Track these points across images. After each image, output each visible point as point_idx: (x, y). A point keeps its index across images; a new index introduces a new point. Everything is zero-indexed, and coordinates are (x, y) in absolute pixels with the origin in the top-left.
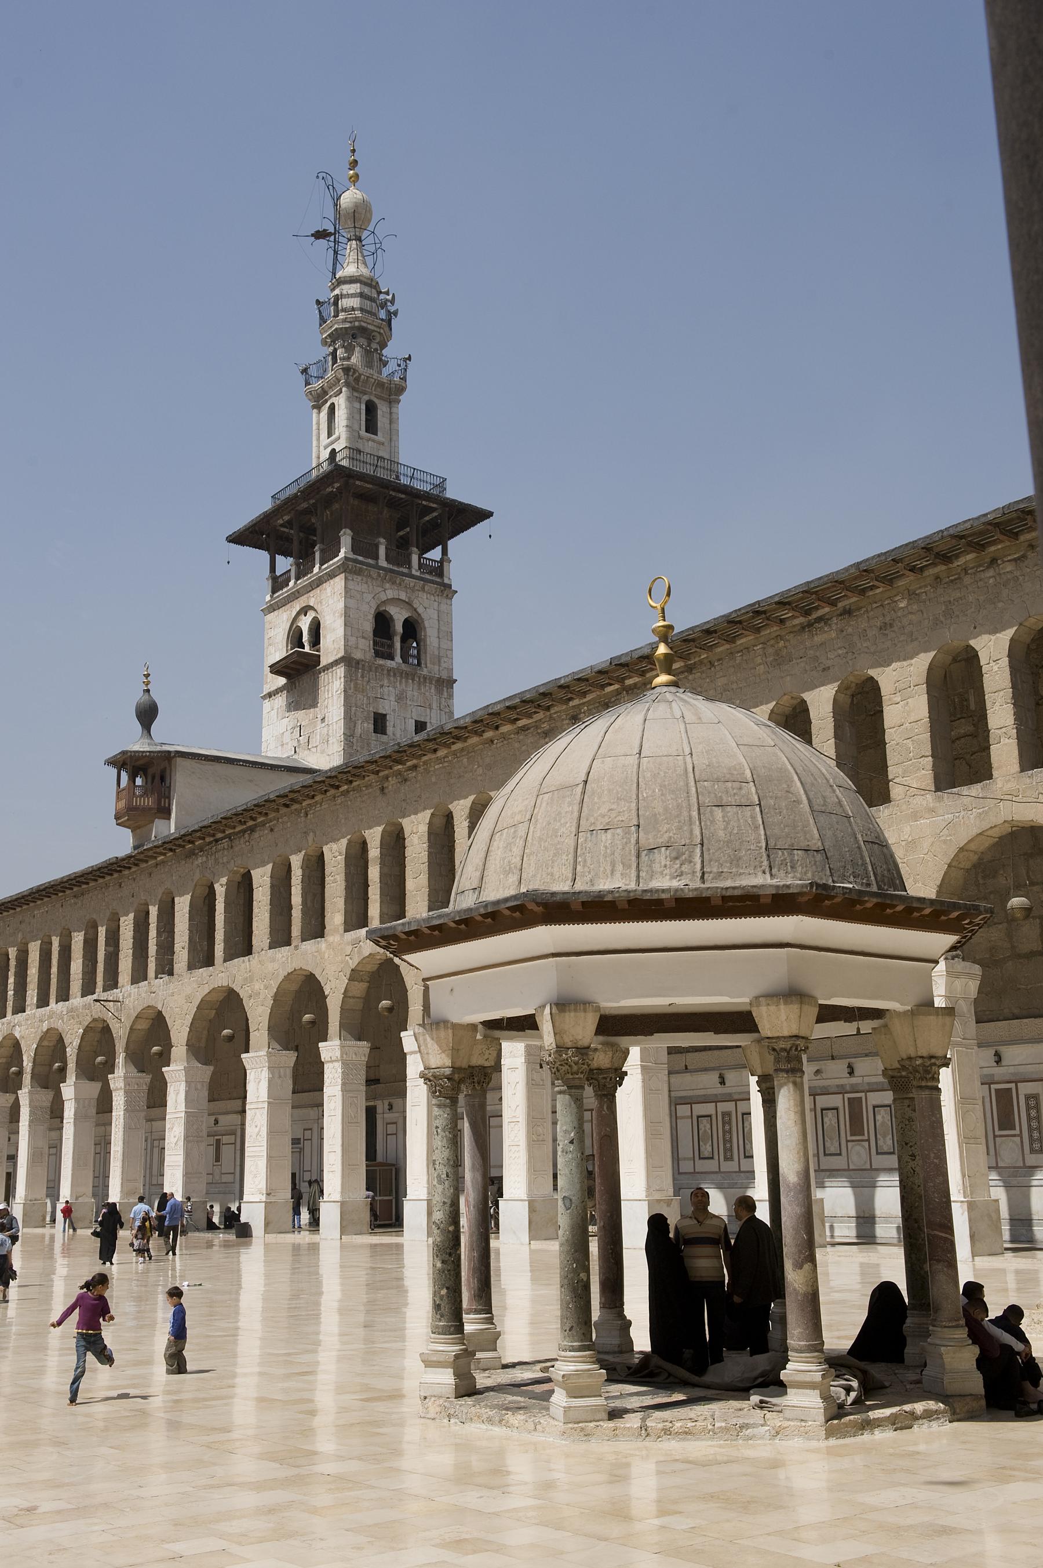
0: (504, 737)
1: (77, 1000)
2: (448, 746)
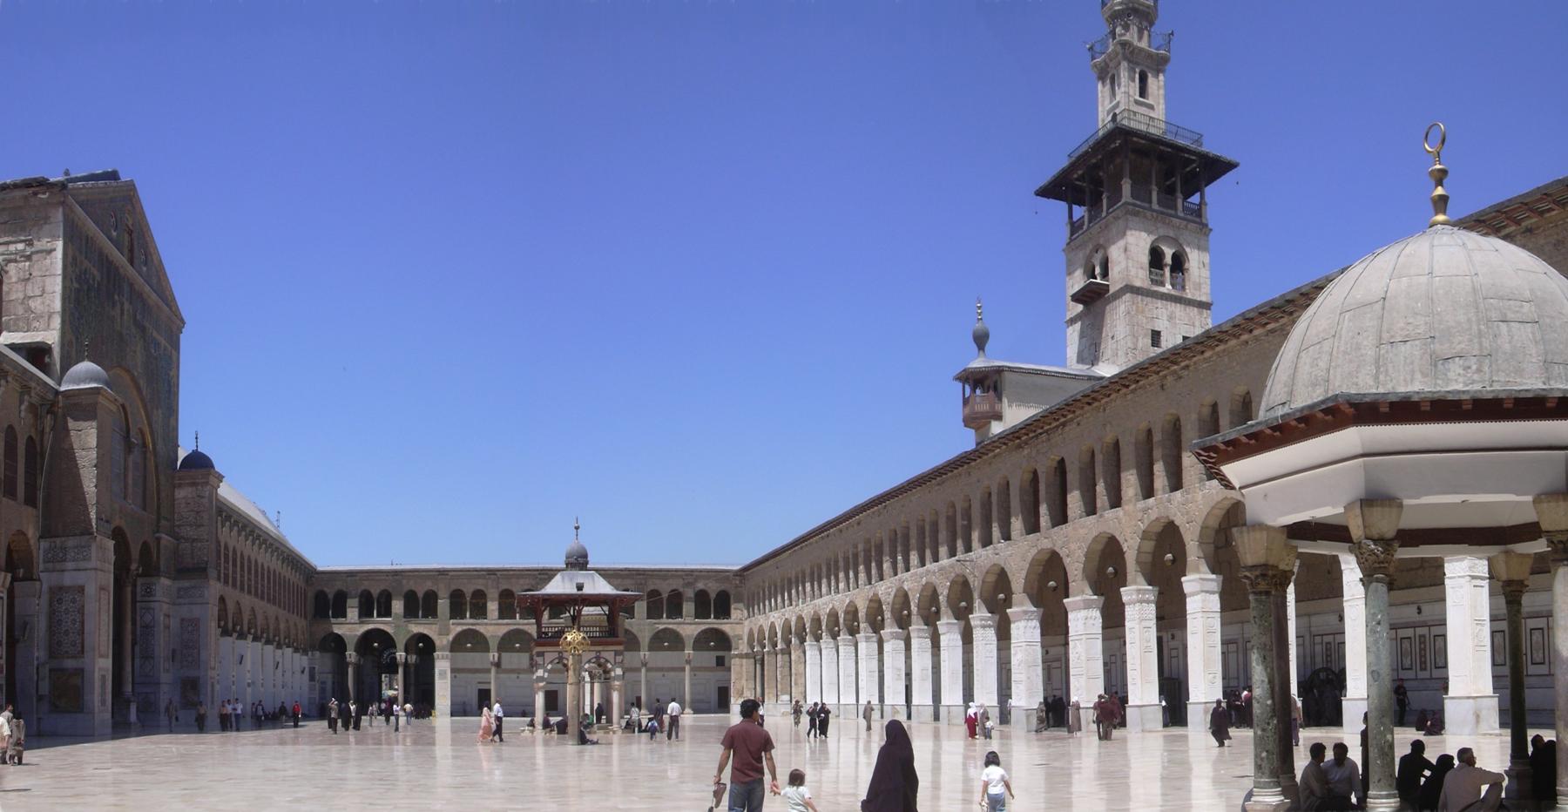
0: (1257, 339)
1: (945, 562)
2: (1212, 348)
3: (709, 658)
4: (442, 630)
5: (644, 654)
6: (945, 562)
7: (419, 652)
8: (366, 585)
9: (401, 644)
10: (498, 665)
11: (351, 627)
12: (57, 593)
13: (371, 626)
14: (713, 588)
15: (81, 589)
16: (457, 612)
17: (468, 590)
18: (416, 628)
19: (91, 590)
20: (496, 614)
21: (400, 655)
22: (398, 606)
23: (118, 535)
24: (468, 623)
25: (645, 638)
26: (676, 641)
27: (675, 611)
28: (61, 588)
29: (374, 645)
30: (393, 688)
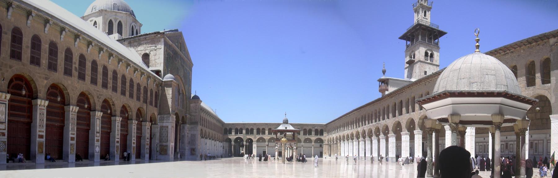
1: (374, 123)
3: (318, 145)
4: (254, 137)
5: (302, 143)
6: (374, 123)
7: (249, 142)
8: (237, 127)
9: (245, 140)
10: (268, 145)
11: (233, 136)
12: (162, 127)
14: (319, 129)
15: (167, 127)
16: (258, 133)
17: (261, 128)
19: (170, 127)
21: (245, 143)
22: (244, 132)
23: (176, 114)
24: (261, 136)
25: (303, 140)
26: (310, 141)
27: (310, 133)
28: (163, 126)
29: (239, 141)
30: (243, 151)
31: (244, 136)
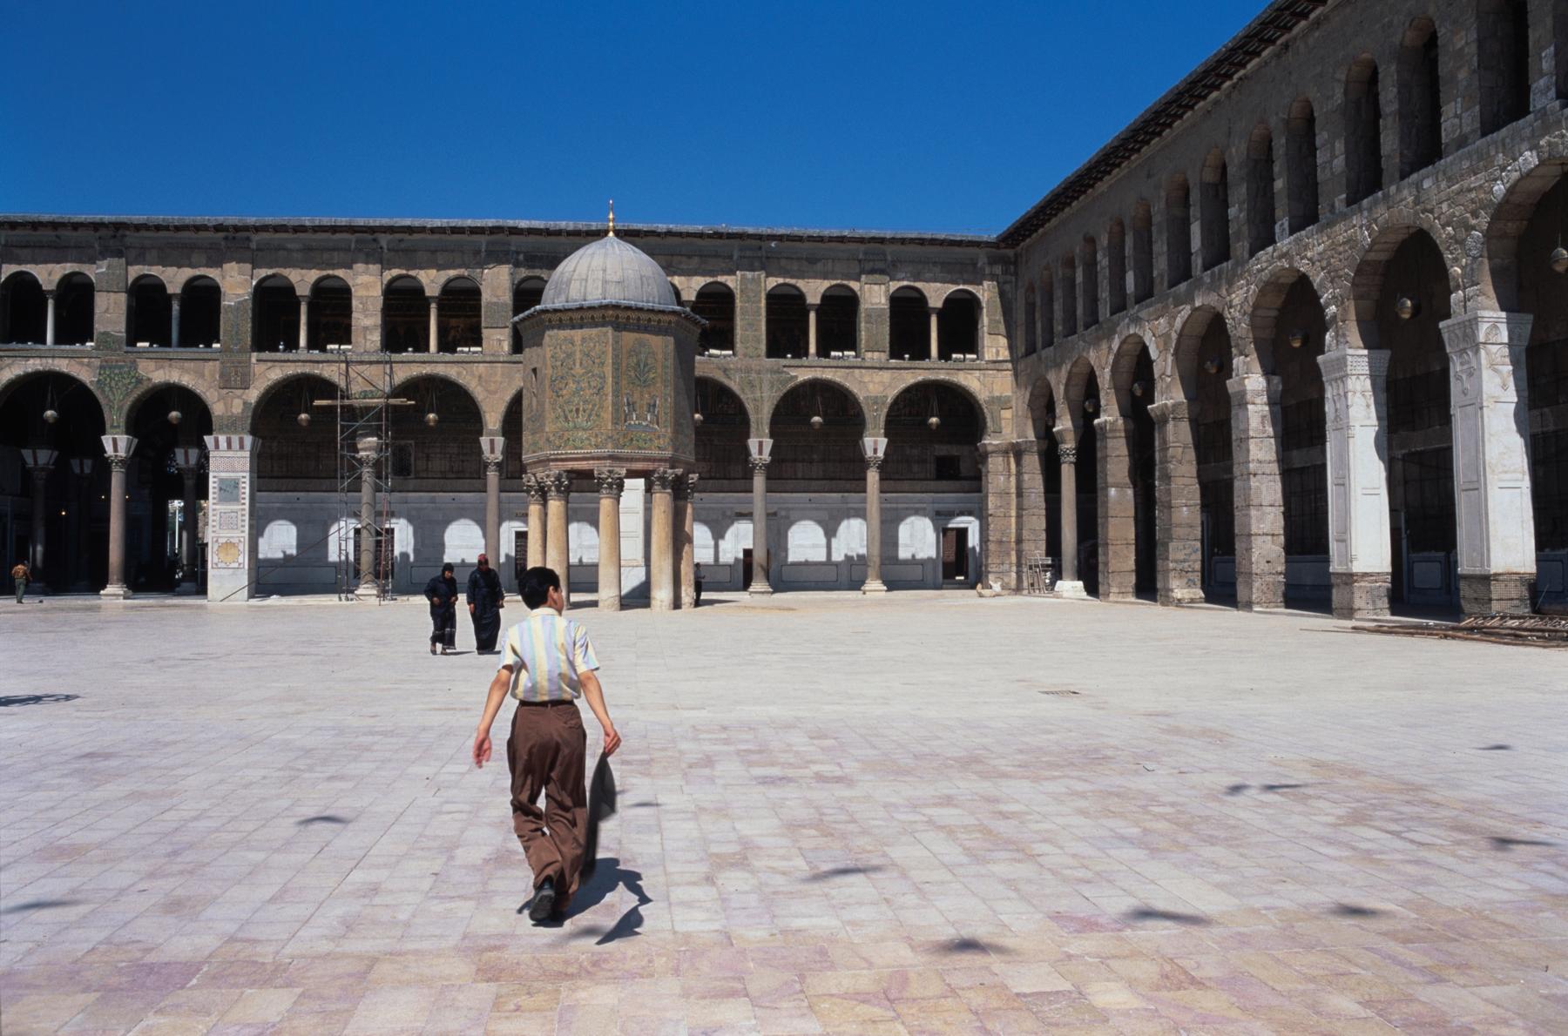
13: (34, 365)
18: (163, 369)
20: (376, 338)
22: (110, 312)
31: (109, 366)
